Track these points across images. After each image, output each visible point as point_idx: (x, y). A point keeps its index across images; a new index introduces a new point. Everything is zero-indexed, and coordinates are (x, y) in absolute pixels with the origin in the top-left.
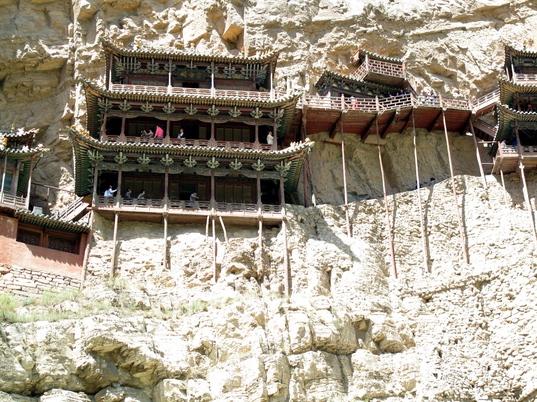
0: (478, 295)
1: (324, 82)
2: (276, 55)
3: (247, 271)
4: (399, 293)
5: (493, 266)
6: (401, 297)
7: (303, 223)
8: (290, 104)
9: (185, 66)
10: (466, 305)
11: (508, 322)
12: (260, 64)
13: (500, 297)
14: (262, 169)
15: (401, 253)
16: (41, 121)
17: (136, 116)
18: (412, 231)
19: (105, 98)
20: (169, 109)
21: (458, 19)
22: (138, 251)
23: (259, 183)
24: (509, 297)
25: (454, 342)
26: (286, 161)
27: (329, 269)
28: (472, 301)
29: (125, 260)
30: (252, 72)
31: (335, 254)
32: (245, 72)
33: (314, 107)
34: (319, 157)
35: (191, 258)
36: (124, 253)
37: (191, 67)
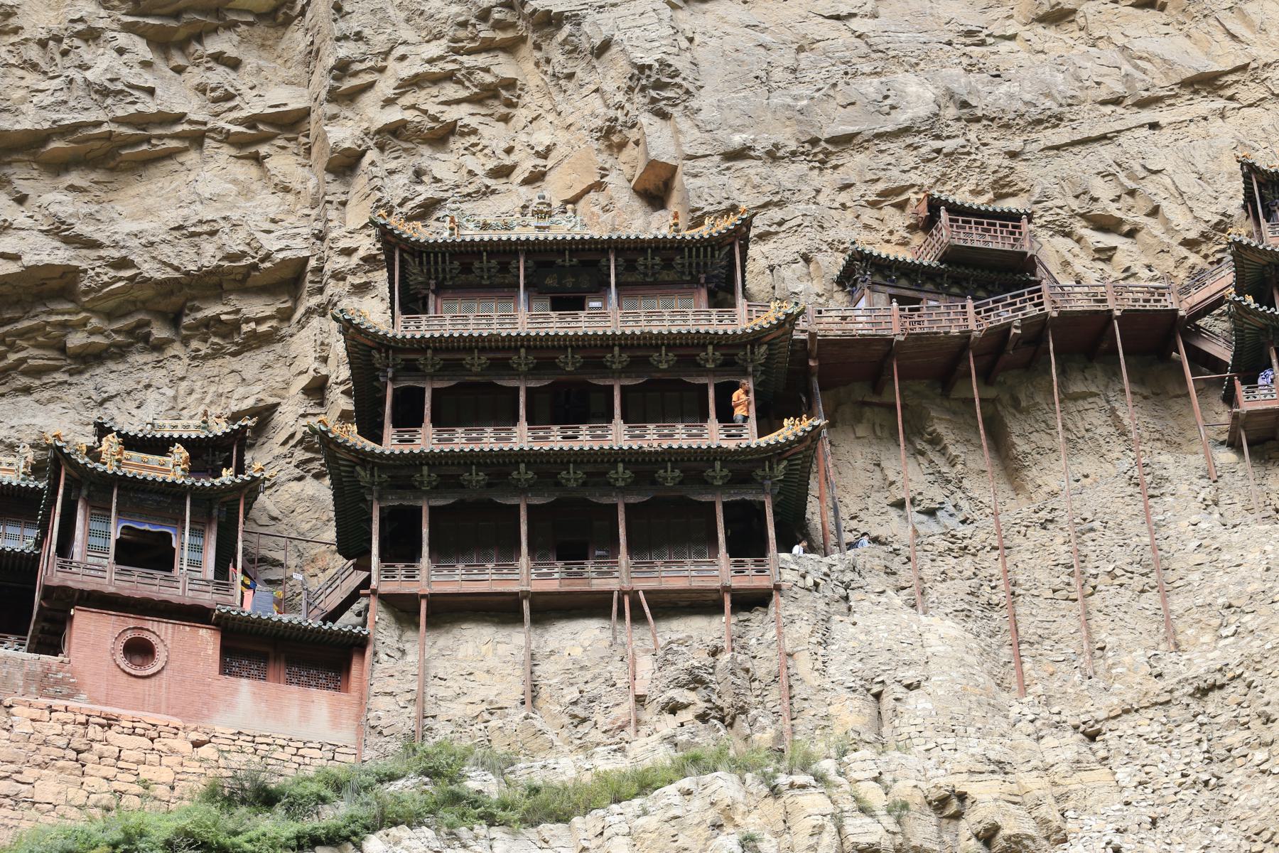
0: (1200, 718)
1: (853, 273)
2: (747, 223)
3: (701, 706)
4: (1031, 728)
5: (1228, 653)
6: (1035, 736)
8: (780, 332)
9: (554, 263)
10: (1175, 743)
11: (1263, 772)
13: (1246, 719)
14: (726, 480)
15: (1036, 637)
16: (260, 396)
17: (452, 383)
18: (1057, 588)
21: (1143, 104)
22: (472, 678)
24: (1264, 719)
25: (1149, 826)
26: (775, 461)
27: (876, 689)
28: (1187, 732)
30: (698, 264)
31: (889, 655)
33: (832, 333)
35: (582, 687)
37: (567, 264)
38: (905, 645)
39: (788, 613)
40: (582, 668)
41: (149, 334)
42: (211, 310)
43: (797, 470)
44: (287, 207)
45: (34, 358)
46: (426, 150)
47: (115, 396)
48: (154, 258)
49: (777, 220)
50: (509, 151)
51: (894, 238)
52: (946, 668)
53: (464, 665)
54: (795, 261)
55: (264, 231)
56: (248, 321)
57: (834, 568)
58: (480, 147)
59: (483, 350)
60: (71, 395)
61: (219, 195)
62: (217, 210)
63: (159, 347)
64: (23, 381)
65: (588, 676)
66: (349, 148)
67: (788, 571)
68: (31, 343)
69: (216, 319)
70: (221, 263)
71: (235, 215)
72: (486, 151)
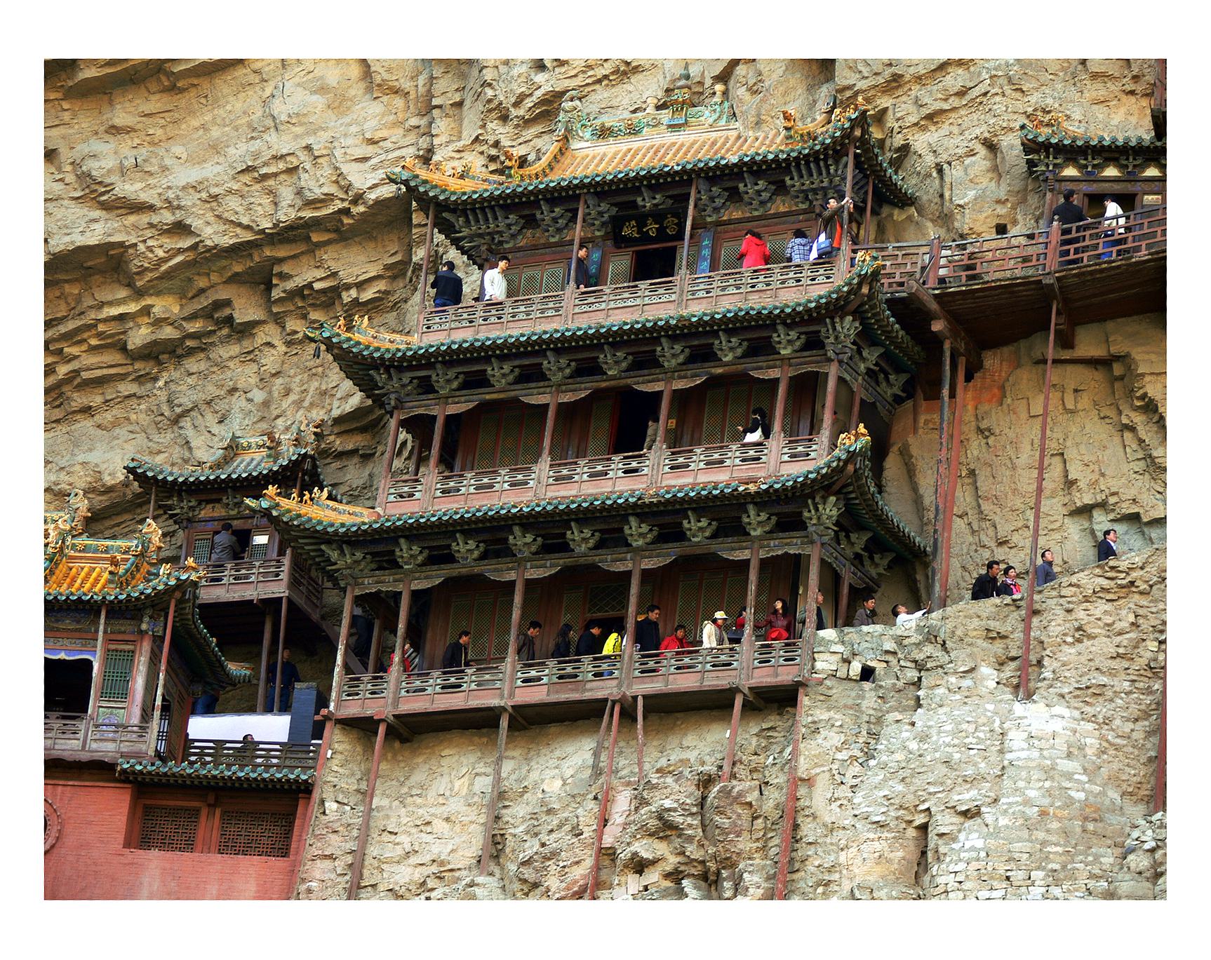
3: (672, 861)
17: (471, 405)
27: (920, 820)
29: (389, 861)
31: (944, 769)
35: (544, 837)
36: (393, 837)
38: (972, 752)
39: (810, 719)
40: (550, 812)
41: (229, 320)
42: (305, 274)
44: (392, 117)
45: (88, 369)
47: (192, 409)
48: (219, 217)
49: (956, 90)
51: (1139, 88)
52: (1021, 784)
53: (421, 811)
54: (972, 153)
56: (348, 287)
57: (906, 642)
59: (503, 358)
60: (140, 414)
61: (297, 115)
62: (297, 137)
63: (246, 330)
64: (79, 400)
67: (826, 656)
68: (84, 347)
69: (309, 286)
70: (299, 214)
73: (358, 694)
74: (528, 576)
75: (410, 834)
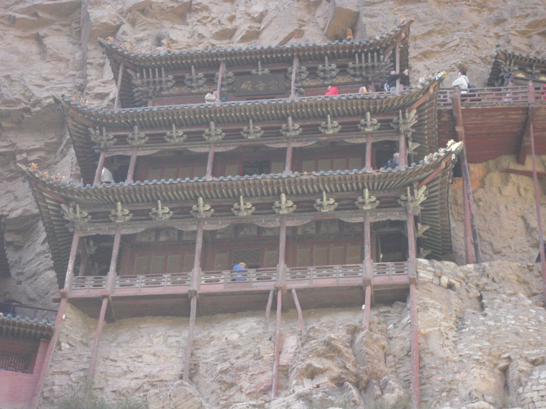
3: (336, 371)
7: (454, 290)
9: (249, 73)
12: (378, 51)
14: (374, 206)
16: (27, 208)
19: (101, 125)
20: (214, 133)
22: (140, 360)
23: (367, 229)
26: (415, 185)
27: (502, 364)
32: (354, 68)
34: (498, 195)
36: (113, 363)
37: (260, 73)
43: (436, 196)
44: (57, 71)
46: (167, 24)
50: (232, 19)
53: (133, 350)
55: (36, 85)
56: (21, 152)
58: (210, 19)
65: (240, 353)
66: (105, 23)
71: (15, 75)
72: (214, 21)
73: (83, 286)
74: (205, 228)
75: (126, 362)
